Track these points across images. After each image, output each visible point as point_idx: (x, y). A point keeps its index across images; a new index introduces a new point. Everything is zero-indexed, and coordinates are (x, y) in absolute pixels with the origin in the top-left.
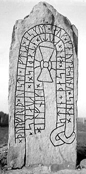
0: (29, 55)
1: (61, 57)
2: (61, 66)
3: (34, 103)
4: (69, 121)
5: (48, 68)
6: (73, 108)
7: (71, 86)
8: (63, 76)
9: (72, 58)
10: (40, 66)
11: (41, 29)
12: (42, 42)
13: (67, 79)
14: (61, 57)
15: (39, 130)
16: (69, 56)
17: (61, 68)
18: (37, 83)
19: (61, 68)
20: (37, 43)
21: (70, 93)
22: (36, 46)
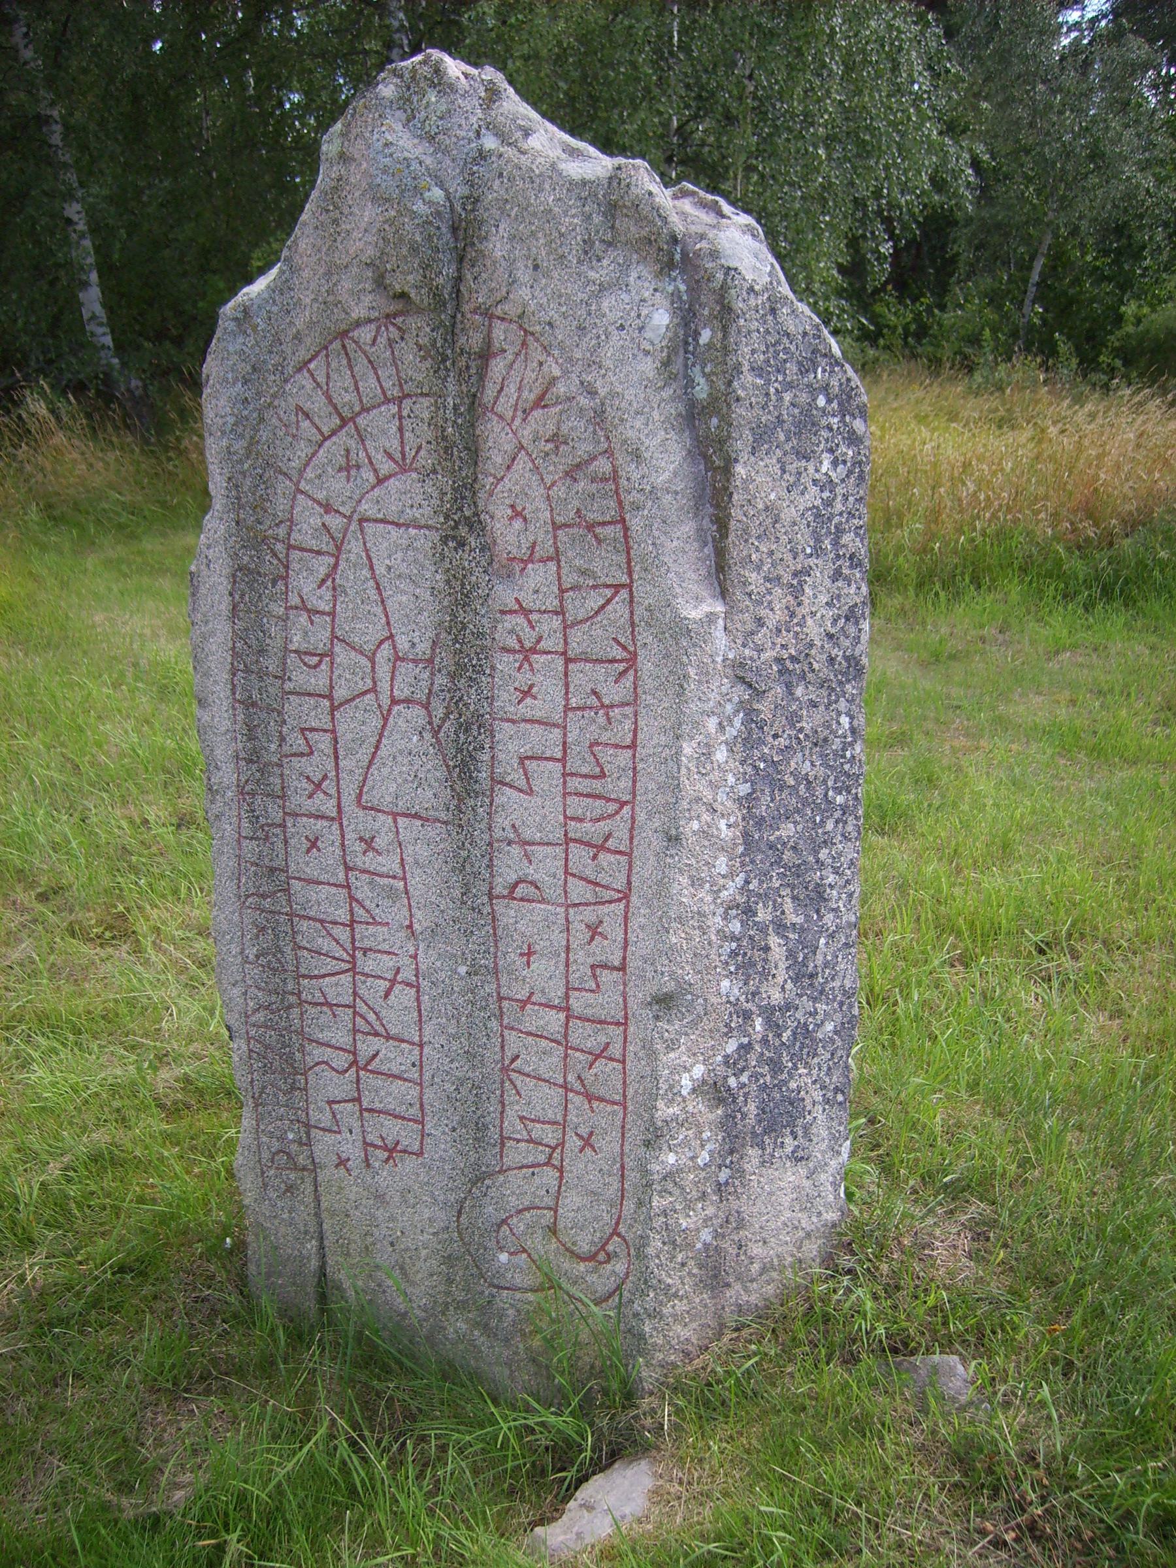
0: (294, 600)
1: (525, 612)
2: (527, 693)
3: (353, 969)
4: (587, 1142)
5: (426, 706)
6: (616, 1050)
7: (611, 869)
8: (547, 775)
9: (618, 607)
10: (373, 690)
11: (361, 365)
12: (380, 481)
13: (576, 806)
14: (525, 612)
15: (392, 1151)
16: (594, 601)
17: (531, 707)
18: (357, 821)
19: (531, 707)
20: (337, 487)
21: (594, 930)
22: (335, 522)
